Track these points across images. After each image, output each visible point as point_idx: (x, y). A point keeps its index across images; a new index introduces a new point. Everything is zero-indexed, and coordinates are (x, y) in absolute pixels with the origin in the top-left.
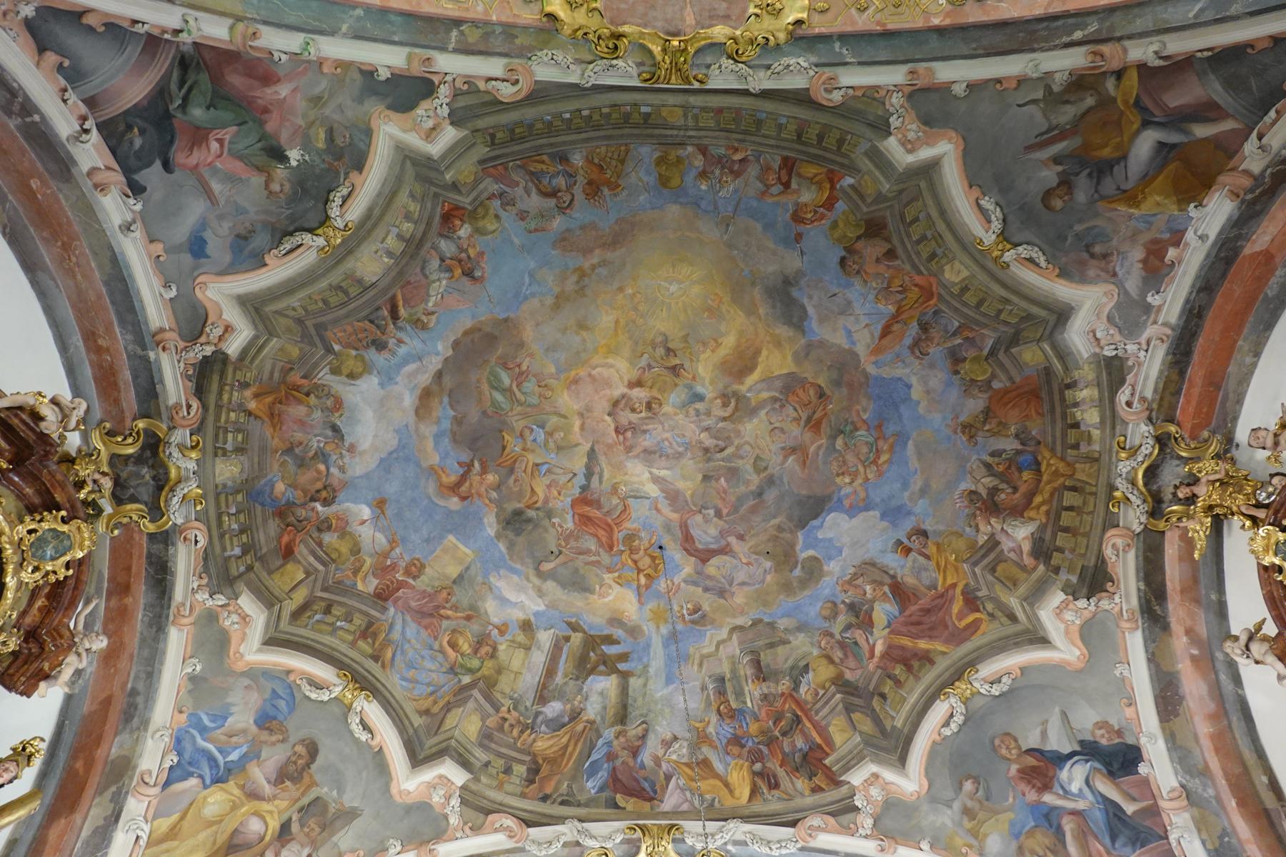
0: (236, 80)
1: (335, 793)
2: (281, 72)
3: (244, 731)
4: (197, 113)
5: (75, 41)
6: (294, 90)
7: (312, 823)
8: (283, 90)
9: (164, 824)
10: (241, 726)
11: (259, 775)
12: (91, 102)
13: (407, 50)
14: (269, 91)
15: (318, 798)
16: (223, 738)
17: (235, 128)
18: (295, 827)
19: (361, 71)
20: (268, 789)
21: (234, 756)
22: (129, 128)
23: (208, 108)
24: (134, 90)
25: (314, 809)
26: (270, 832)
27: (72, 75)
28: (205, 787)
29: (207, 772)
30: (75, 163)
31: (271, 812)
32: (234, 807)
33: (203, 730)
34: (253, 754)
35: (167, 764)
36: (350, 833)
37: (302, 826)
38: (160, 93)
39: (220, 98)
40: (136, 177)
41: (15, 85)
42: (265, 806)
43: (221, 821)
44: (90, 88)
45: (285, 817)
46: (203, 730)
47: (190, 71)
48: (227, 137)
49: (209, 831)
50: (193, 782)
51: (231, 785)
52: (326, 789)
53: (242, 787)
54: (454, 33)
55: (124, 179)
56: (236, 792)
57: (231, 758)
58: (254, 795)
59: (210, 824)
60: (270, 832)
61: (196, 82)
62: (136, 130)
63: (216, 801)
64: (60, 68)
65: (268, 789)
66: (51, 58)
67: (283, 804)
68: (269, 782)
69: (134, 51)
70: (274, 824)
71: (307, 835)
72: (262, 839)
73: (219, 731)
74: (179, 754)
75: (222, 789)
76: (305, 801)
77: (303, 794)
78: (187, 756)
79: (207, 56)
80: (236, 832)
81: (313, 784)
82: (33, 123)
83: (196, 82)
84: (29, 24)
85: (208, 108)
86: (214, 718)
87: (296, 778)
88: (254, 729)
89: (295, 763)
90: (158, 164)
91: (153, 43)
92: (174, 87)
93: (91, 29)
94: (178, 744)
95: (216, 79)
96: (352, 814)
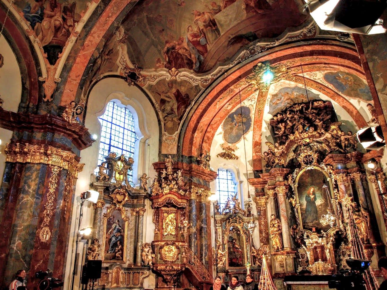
1: (66, 3)
3: (36, 6)
7: (68, 13)
9: (40, 35)
10: (34, 5)
11: (48, 12)
15: (64, 7)
16: (34, 10)
18: (65, 17)
20: (53, 13)
21: (40, 12)
25: (66, 10)
26: (61, 22)
28: (41, 23)
29: (37, 19)
31: (58, 18)
32: (50, 22)
33: (29, 12)
34: (42, 9)
35: (29, 25)
36: (77, 8)
37: (66, 15)
42: (55, 17)
43: (50, 27)
45: (61, 16)
46: (29, 12)
49: (50, 31)
50: (37, 24)
51: (45, 18)
52: (64, 4)
53: (48, 17)
56: (47, 19)
57: (39, 13)
58: (51, 17)
59: (49, 29)
60: (61, 22)
63: (45, 23)
65: (53, 13)
67: (58, 14)
68: (51, 12)
70: (60, 19)
71: (69, 16)
72: (61, 24)
73: (32, 10)
74: (29, 20)
75: (45, 21)
76: (62, 9)
77: (61, 8)
78: (31, 20)
80: (55, 27)
81: (61, 4)
86: (28, 8)
87: (56, 6)
88: (37, 3)
89: (52, 3)
94: (27, 19)
96: (74, 5)
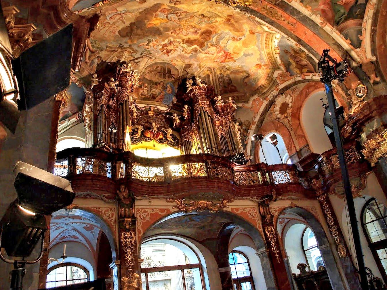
0: (330, 15)
2: (320, 12)
4: (342, 11)
5: (354, 38)
6: (319, 6)
8: (322, 7)
12: (361, 25)
13: (290, 4)
14: (325, 9)
17: (338, 3)
19: (303, 3)
22: (357, 15)
23: (340, 11)
24: (351, 22)
27: (360, 33)
30: (374, 13)
38: (346, 19)
39: (335, 11)
40: (365, 3)
41: (371, 37)
44: (359, 28)
47: (338, 21)
48: (340, 2)
54: (277, 3)
55: (368, 4)
61: (338, 18)
62: (357, 13)
64: (361, 35)
66: (361, 38)
69: (345, 31)
79: (332, 23)
82: (374, 27)
83: (338, 18)
84: (360, 46)
85: (340, 11)
90: (358, 3)
91: (341, 31)
92: (343, 19)
93: (350, 40)
95: (334, 16)
